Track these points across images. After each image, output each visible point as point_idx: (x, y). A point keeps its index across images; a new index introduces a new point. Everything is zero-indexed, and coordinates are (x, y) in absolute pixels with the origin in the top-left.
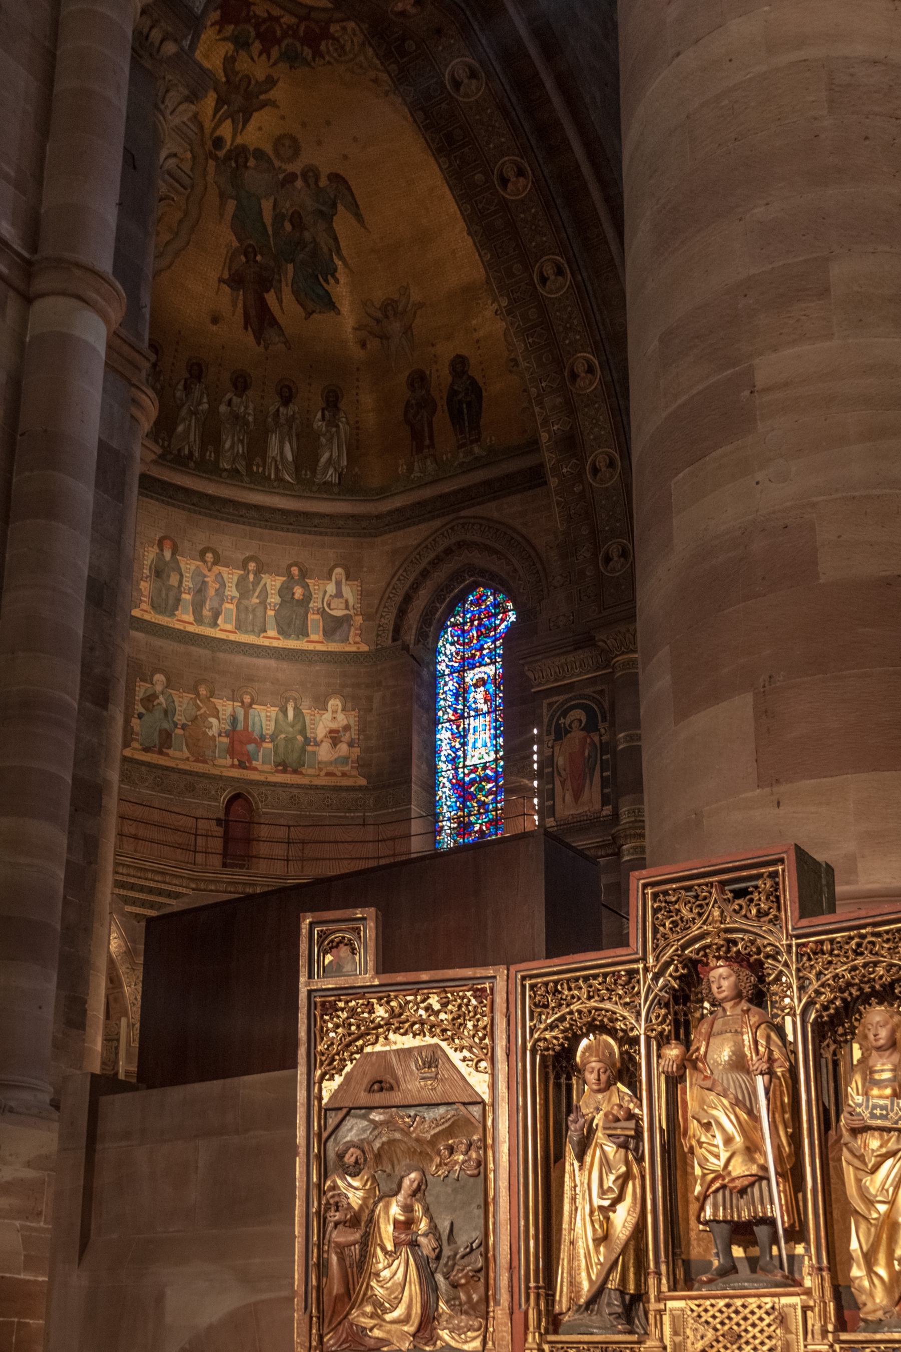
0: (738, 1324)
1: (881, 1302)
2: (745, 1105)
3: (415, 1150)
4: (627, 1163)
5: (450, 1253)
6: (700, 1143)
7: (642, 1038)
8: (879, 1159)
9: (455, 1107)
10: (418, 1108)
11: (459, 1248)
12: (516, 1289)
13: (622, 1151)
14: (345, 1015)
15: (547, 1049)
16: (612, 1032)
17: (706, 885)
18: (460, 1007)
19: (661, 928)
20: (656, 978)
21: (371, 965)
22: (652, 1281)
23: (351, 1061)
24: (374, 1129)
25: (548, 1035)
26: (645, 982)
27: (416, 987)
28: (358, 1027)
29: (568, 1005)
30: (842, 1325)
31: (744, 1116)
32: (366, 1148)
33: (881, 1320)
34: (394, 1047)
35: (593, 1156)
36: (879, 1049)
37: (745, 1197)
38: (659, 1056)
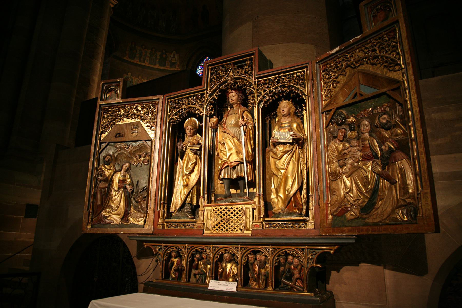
0: (229, 215)
1: (281, 207)
4: (196, 159)
7: (204, 116)
10: (131, 143)
11: (139, 189)
12: (156, 203)
13: (196, 155)
15: (174, 122)
22: (201, 200)
23: (111, 127)
24: (116, 149)
27: (133, 103)
28: (114, 116)
29: (181, 107)
30: (266, 215)
32: (113, 156)
33: (280, 213)
34: (125, 123)
35: (186, 158)
37: (235, 169)
38: (209, 122)
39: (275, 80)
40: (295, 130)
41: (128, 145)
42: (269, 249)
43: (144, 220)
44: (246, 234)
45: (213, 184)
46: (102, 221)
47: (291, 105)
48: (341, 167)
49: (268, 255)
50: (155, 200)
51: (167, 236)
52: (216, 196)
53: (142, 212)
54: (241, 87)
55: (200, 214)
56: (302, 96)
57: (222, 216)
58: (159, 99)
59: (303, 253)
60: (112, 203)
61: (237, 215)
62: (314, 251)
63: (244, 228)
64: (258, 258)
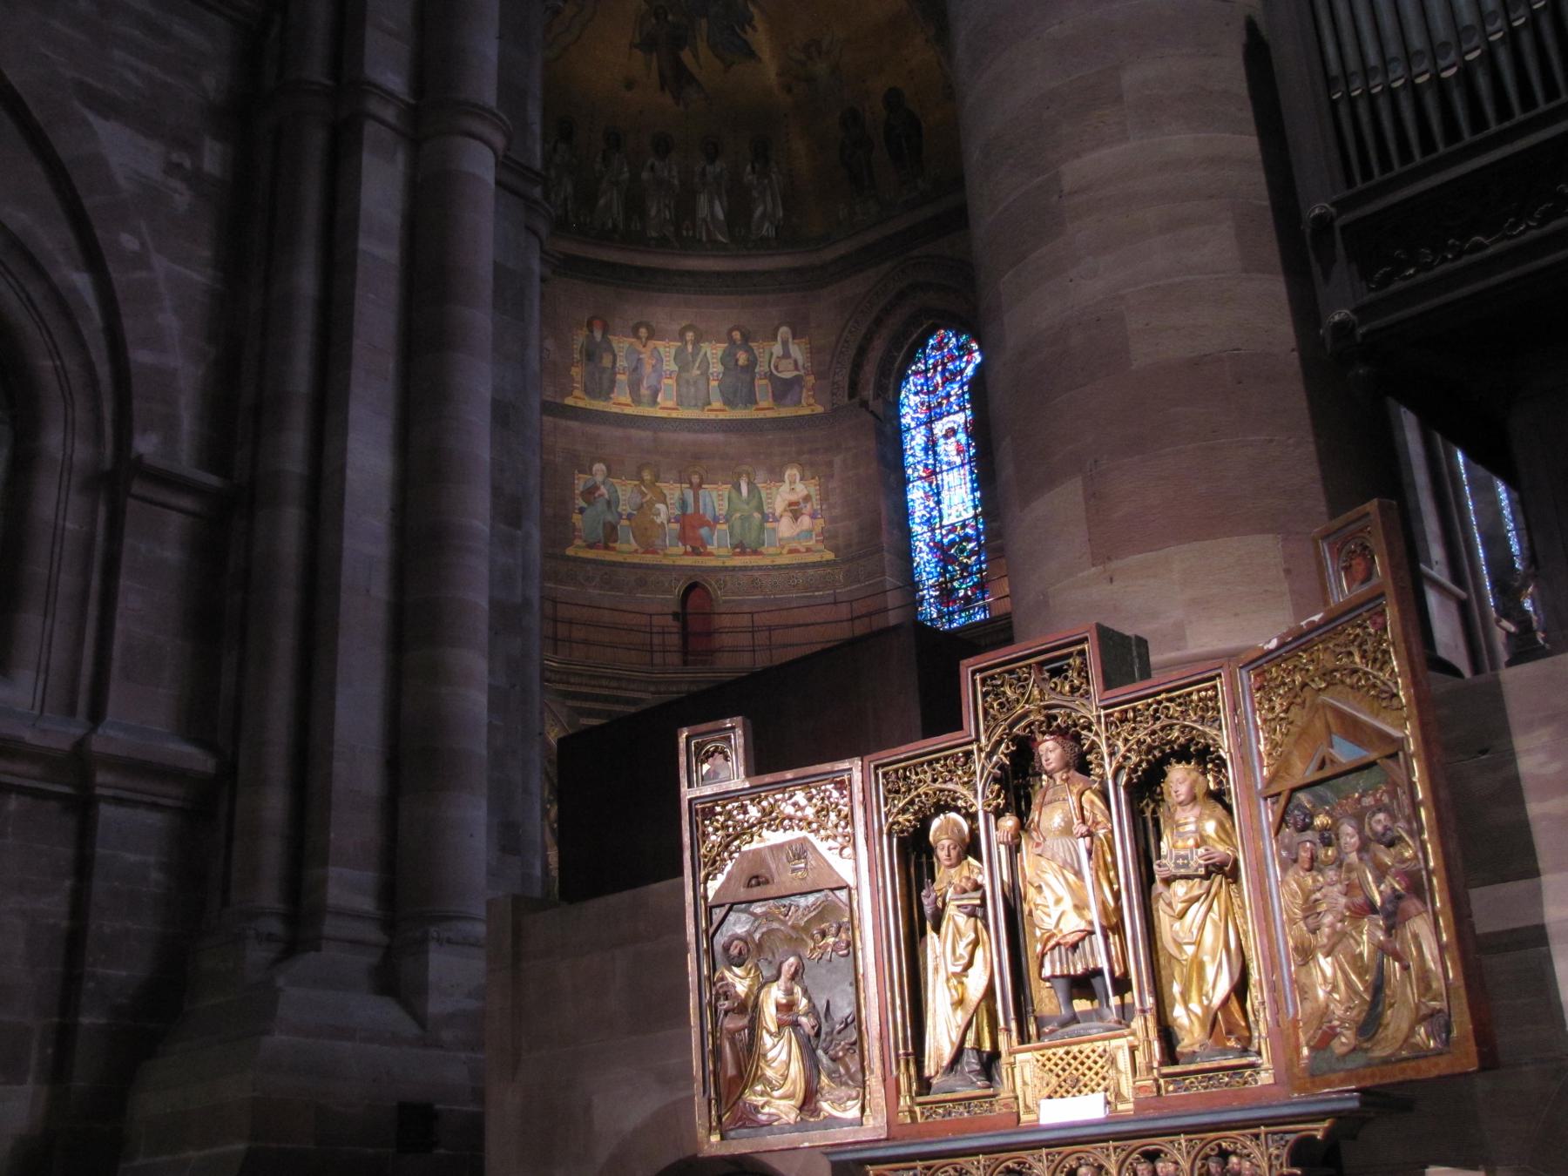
0: (1077, 1069)
2: (1073, 867)
3: (792, 937)
5: (829, 1030)
6: (1037, 905)
8: (1184, 905)
9: (823, 893)
10: (792, 898)
12: (887, 1057)
13: (972, 919)
14: (721, 819)
15: (902, 831)
16: (957, 810)
17: (1026, 666)
18: (823, 799)
19: (991, 710)
20: (989, 756)
21: (742, 769)
22: (1002, 1039)
23: (731, 859)
24: (754, 921)
25: (901, 818)
26: (979, 761)
27: (782, 786)
28: (734, 828)
29: (916, 789)
31: (1071, 877)
32: (749, 940)
34: (768, 843)
36: (1180, 803)
38: (997, 829)
39: (1148, 710)
40: (1213, 839)
41: (785, 906)
42: (1180, 1144)
43: (859, 1105)
44: (1122, 1111)
45: (1028, 991)
46: (748, 1119)
47: (1194, 774)
48: (1314, 932)
49: (1179, 1158)
50: (882, 1050)
51: (928, 1139)
52: (1040, 1022)
53: (851, 1083)
54: (1068, 727)
55: (1004, 1074)
56: (1217, 751)
57: (1061, 1073)
58: (851, 769)
59: (1258, 1145)
60: (767, 1069)
61: (1096, 1068)
62: (1282, 1139)
63: (1116, 1098)
64: (1159, 1170)
